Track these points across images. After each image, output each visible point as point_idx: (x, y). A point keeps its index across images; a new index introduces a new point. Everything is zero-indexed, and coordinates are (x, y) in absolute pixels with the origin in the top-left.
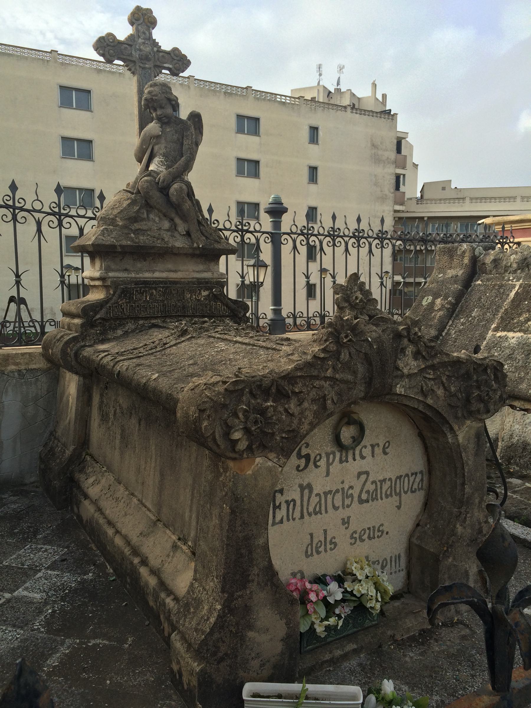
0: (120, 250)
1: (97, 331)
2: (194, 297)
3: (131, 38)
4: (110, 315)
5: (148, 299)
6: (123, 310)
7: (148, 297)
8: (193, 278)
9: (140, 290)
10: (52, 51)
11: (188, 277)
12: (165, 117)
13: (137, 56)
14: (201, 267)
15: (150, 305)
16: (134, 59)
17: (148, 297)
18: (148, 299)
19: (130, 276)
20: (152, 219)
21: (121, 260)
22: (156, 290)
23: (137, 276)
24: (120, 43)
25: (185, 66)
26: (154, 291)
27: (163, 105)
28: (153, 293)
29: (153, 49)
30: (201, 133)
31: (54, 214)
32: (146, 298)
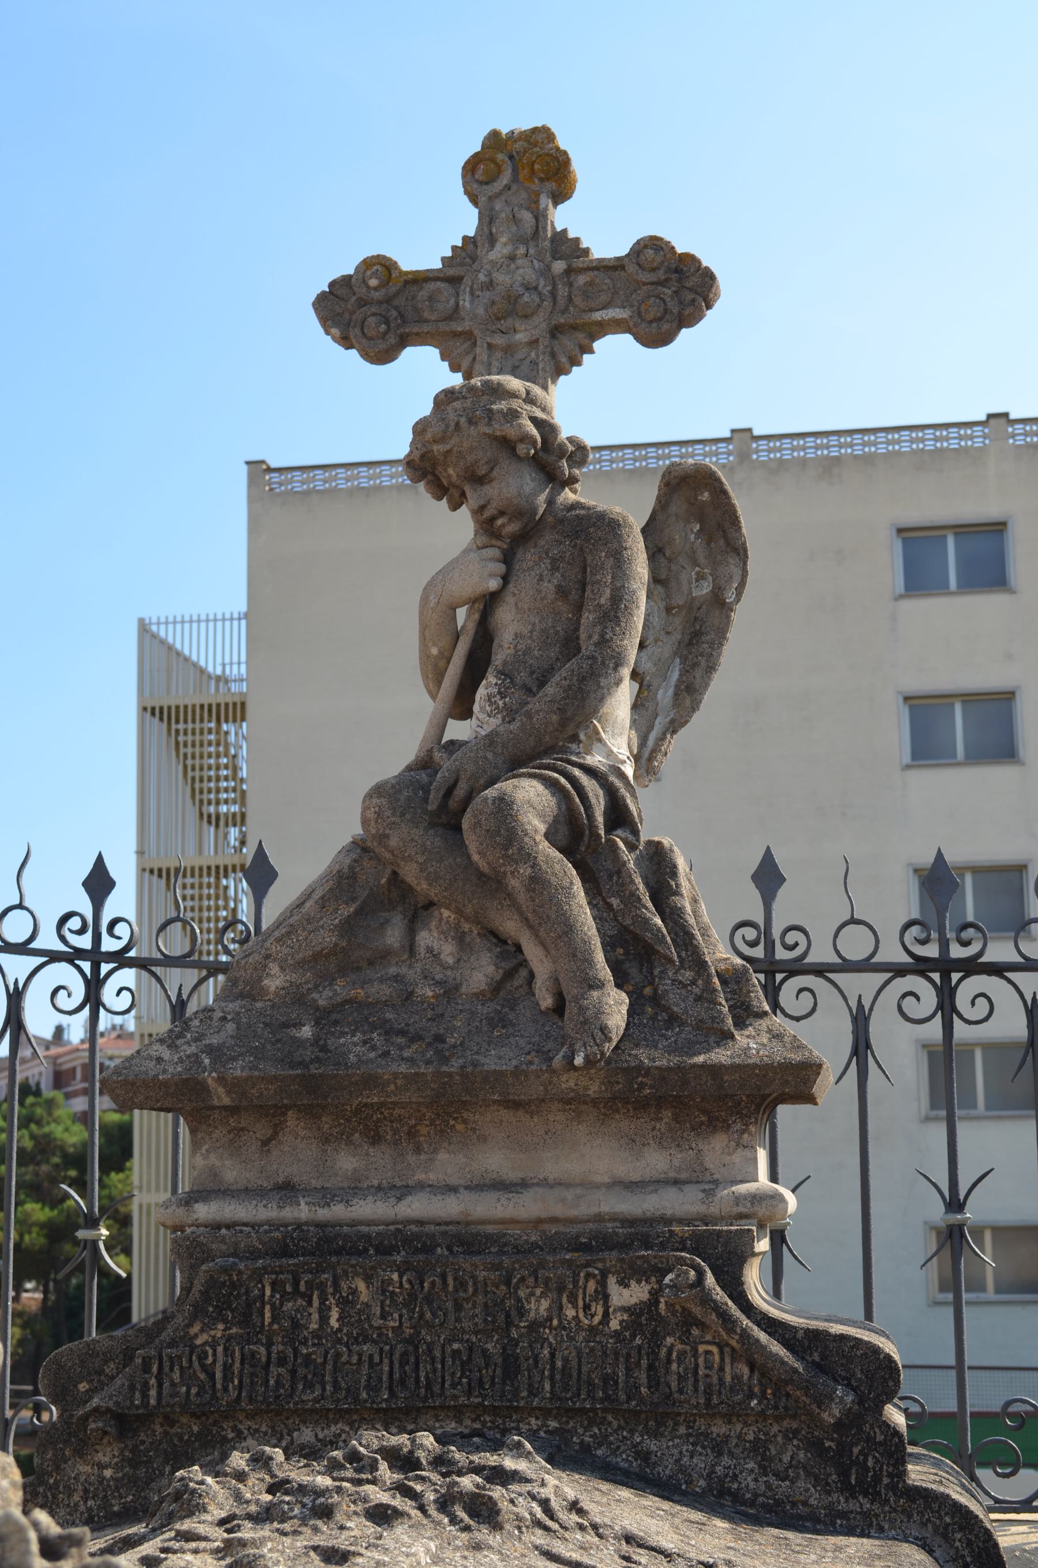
0: (226, 1101)
1: (101, 1467)
2: (570, 1313)
3: (466, 253)
4: (145, 1396)
5: (334, 1323)
6: (212, 1376)
7: (335, 1314)
8: (599, 1218)
9: (296, 1283)
10: (990, 416)
11: (573, 1213)
12: (502, 513)
13: (481, 311)
14: (657, 1161)
15: (338, 1355)
16: (466, 325)
17: (335, 1314)
18: (334, 1323)
19: (289, 1213)
20: (429, 950)
21: (266, 1143)
22: (368, 1279)
23: (323, 1214)
24: (419, 279)
25: (689, 296)
26: (361, 1286)
27: (482, 471)
28: (354, 1292)
29: (548, 268)
30: (740, 552)
31: (921, 967)
32: (324, 1319)
